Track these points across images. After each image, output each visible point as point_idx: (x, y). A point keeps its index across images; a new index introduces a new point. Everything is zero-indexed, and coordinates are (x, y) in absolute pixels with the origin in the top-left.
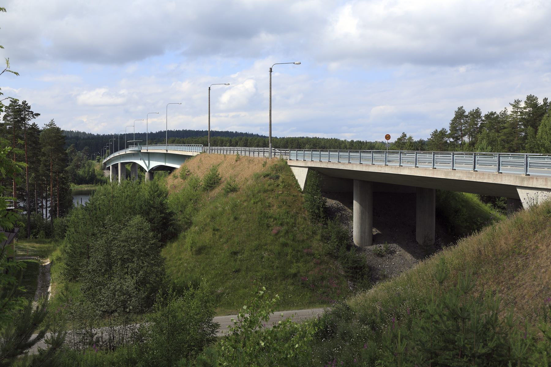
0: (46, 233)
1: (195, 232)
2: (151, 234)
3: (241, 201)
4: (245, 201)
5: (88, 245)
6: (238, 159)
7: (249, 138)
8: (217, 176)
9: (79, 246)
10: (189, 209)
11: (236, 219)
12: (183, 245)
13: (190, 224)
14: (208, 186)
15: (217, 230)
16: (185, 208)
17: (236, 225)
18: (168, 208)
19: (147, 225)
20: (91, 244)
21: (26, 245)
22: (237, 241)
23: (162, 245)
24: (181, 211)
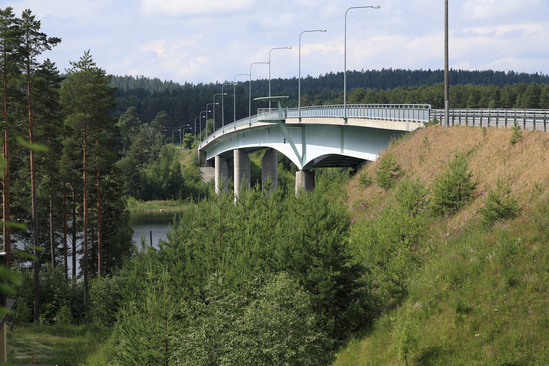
0: (73, 310)
1: (413, 315)
2: (311, 319)
3: (524, 241)
4: (536, 240)
5: (166, 341)
6: (517, 138)
7: (544, 88)
8: (465, 180)
9: (146, 343)
10: (398, 261)
11: (512, 283)
12: (385, 345)
13: (400, 295)
14: (444, 203)
15: (468, 311)
16: (389, 256)
17: (512, 300)
18: (350, 257)
19: (302, 298)
20: (173, 340)
21: (30, 337)
22: (514, 336)
23: (335, 344)
24: (380, 264)
